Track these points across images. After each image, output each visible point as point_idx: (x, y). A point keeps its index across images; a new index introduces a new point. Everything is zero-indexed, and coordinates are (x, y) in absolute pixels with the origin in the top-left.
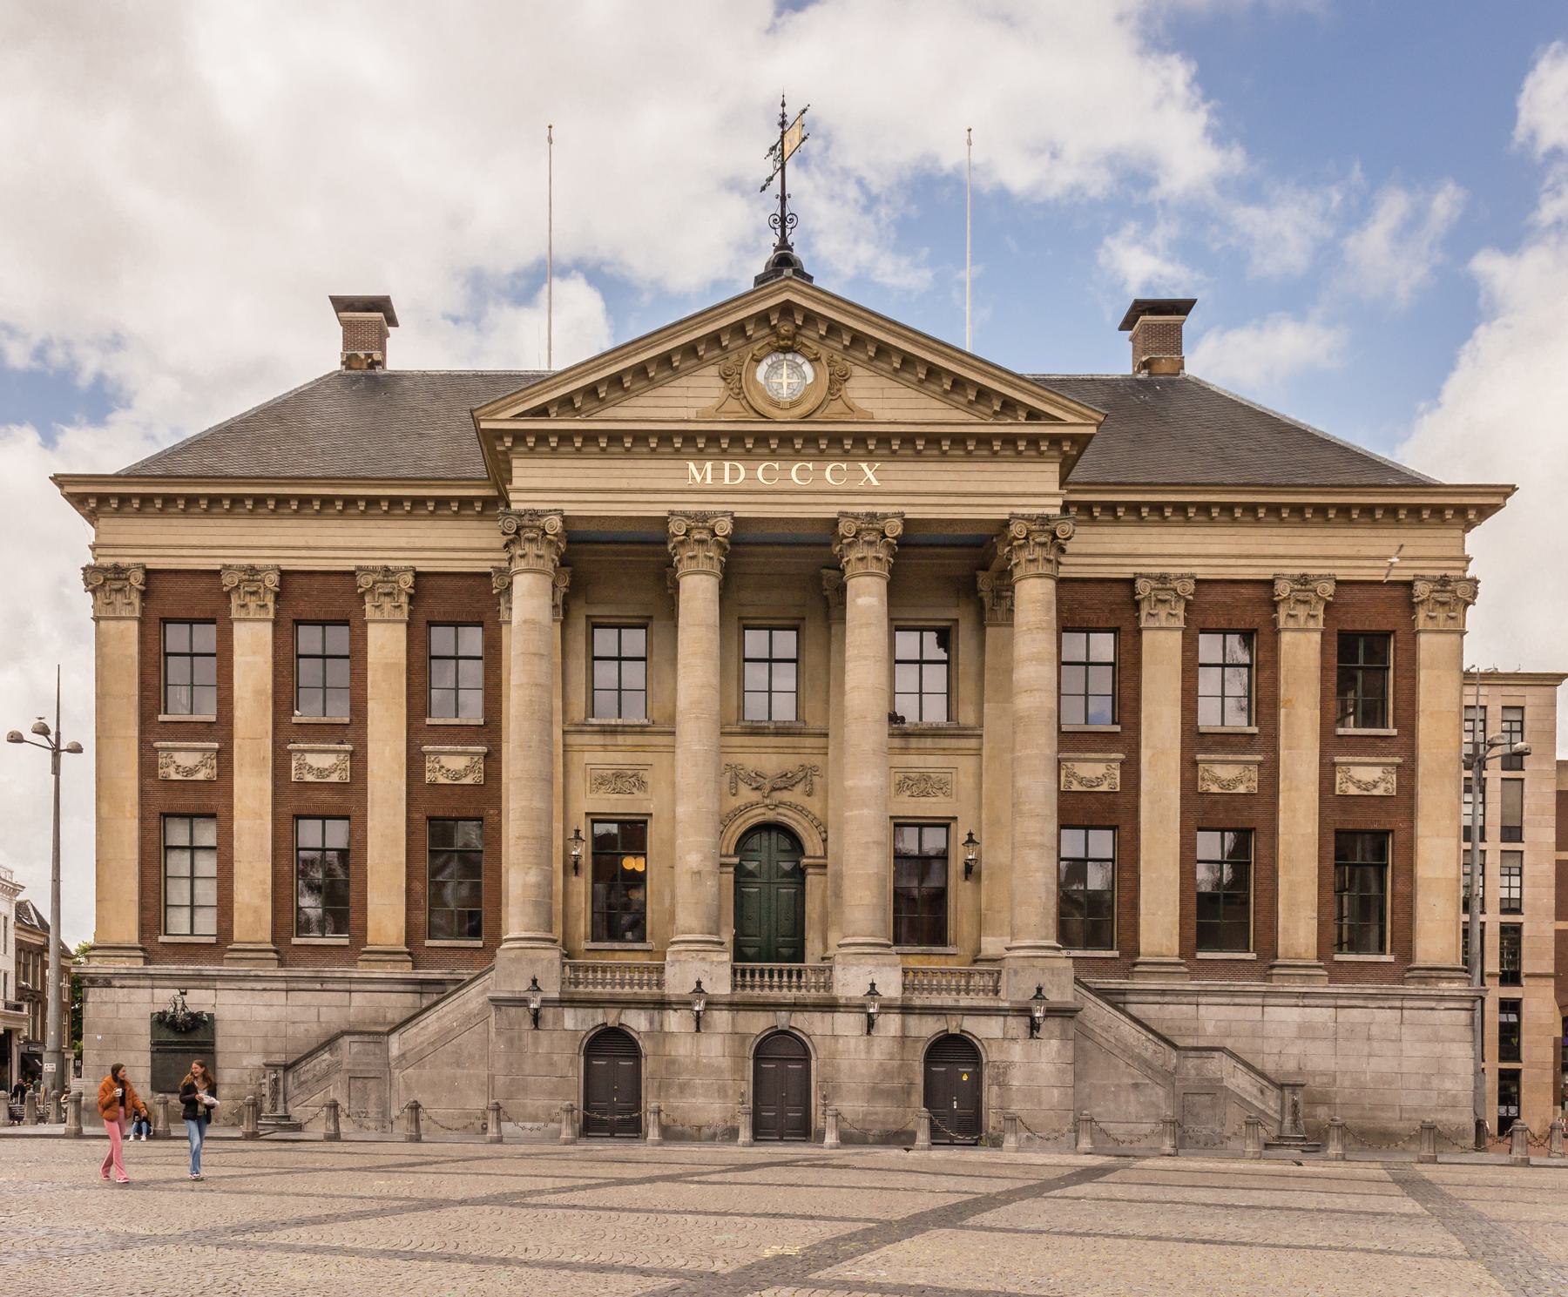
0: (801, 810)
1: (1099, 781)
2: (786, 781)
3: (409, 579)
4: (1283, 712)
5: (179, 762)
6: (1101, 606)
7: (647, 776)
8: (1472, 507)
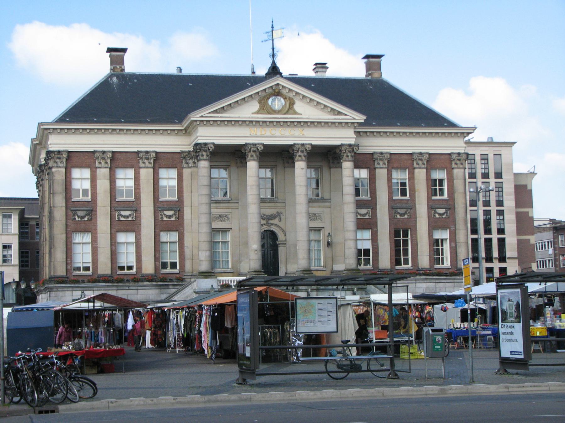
0: (277, 226)
1: (365, 214)
2: (273, 217)
3: (154, 154)
4: (416, 193)
5: (79, 214)
6: (363, 160)
7: (230, 216)
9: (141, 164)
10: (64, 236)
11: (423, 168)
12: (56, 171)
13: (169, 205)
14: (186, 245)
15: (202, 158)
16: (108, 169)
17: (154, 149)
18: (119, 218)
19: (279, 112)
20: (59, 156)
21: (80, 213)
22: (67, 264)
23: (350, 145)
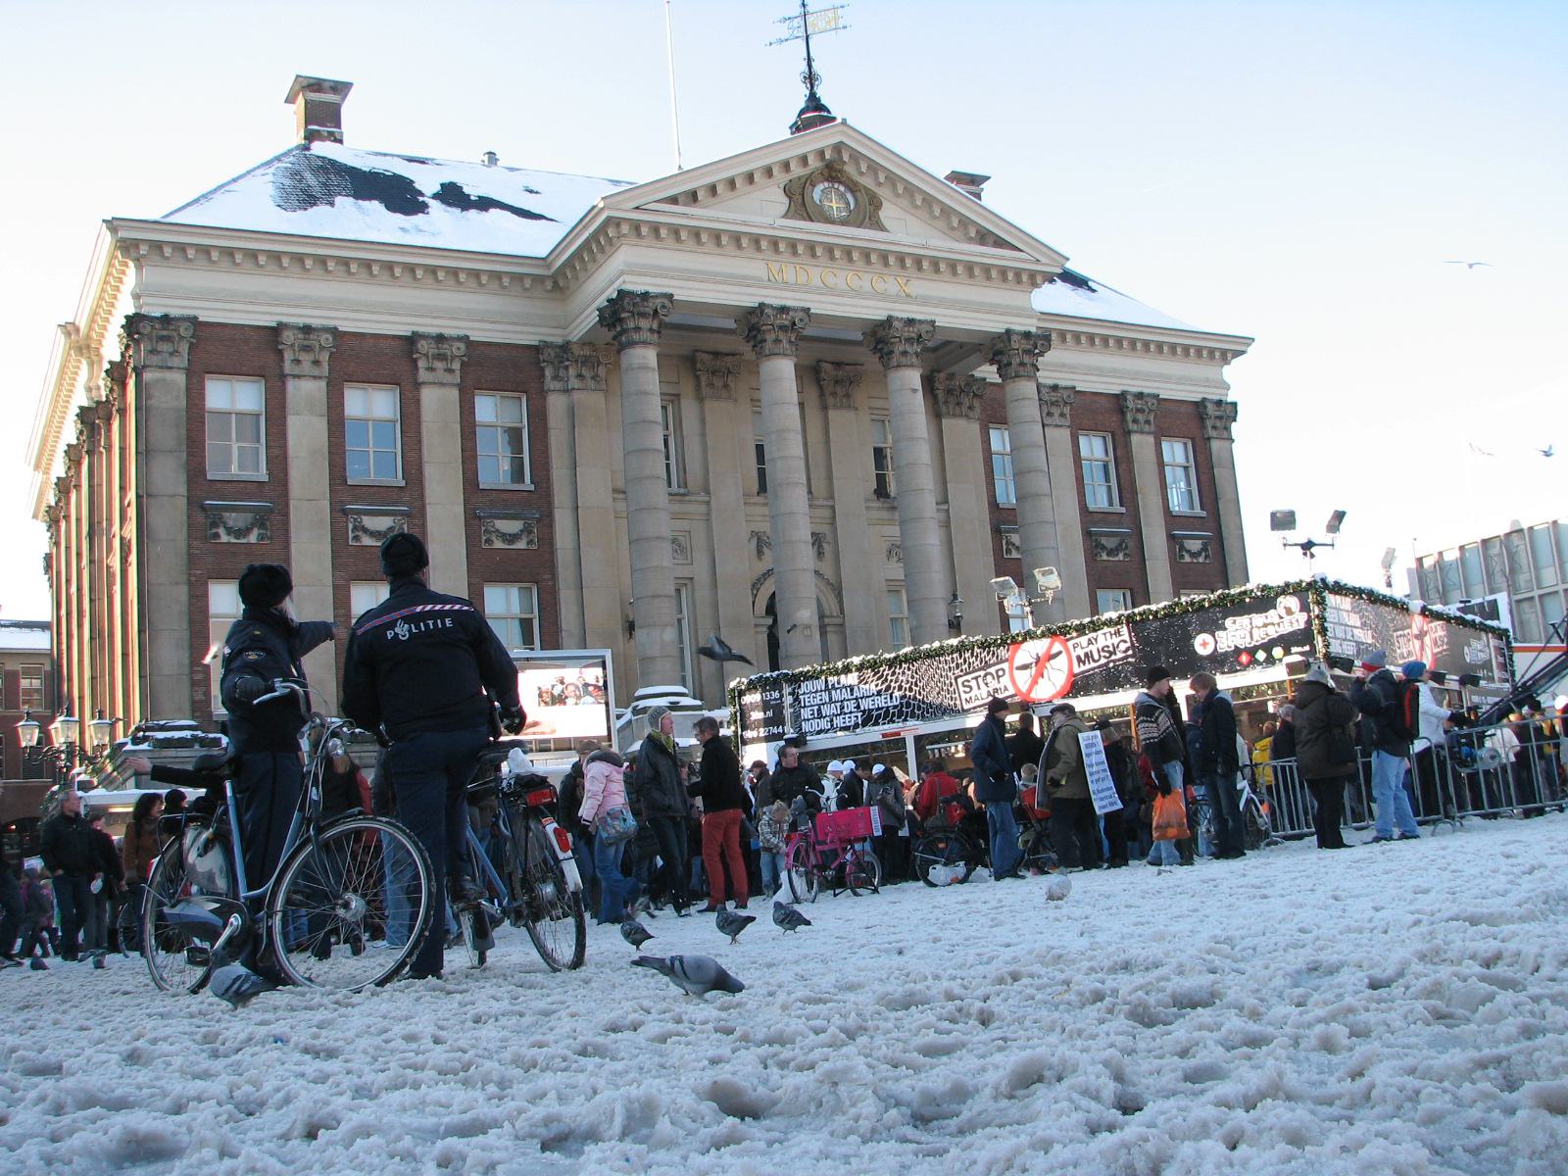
3: (462, 346)
5: (231, 523)
8: (1225, 350)
9: (423, 375)
10: (184, 590)
11: (1148, 433)
12: (157, 381)
13: (501, 502)
14: (564, 626)
15: (636, 337)
16: (323, 384)
17: (462, 333)
18: (356, 538)
19: (844, 223)
20: (165, 333)
21: (234, 519)
22: (194, 684)
23: (1027, 335)
